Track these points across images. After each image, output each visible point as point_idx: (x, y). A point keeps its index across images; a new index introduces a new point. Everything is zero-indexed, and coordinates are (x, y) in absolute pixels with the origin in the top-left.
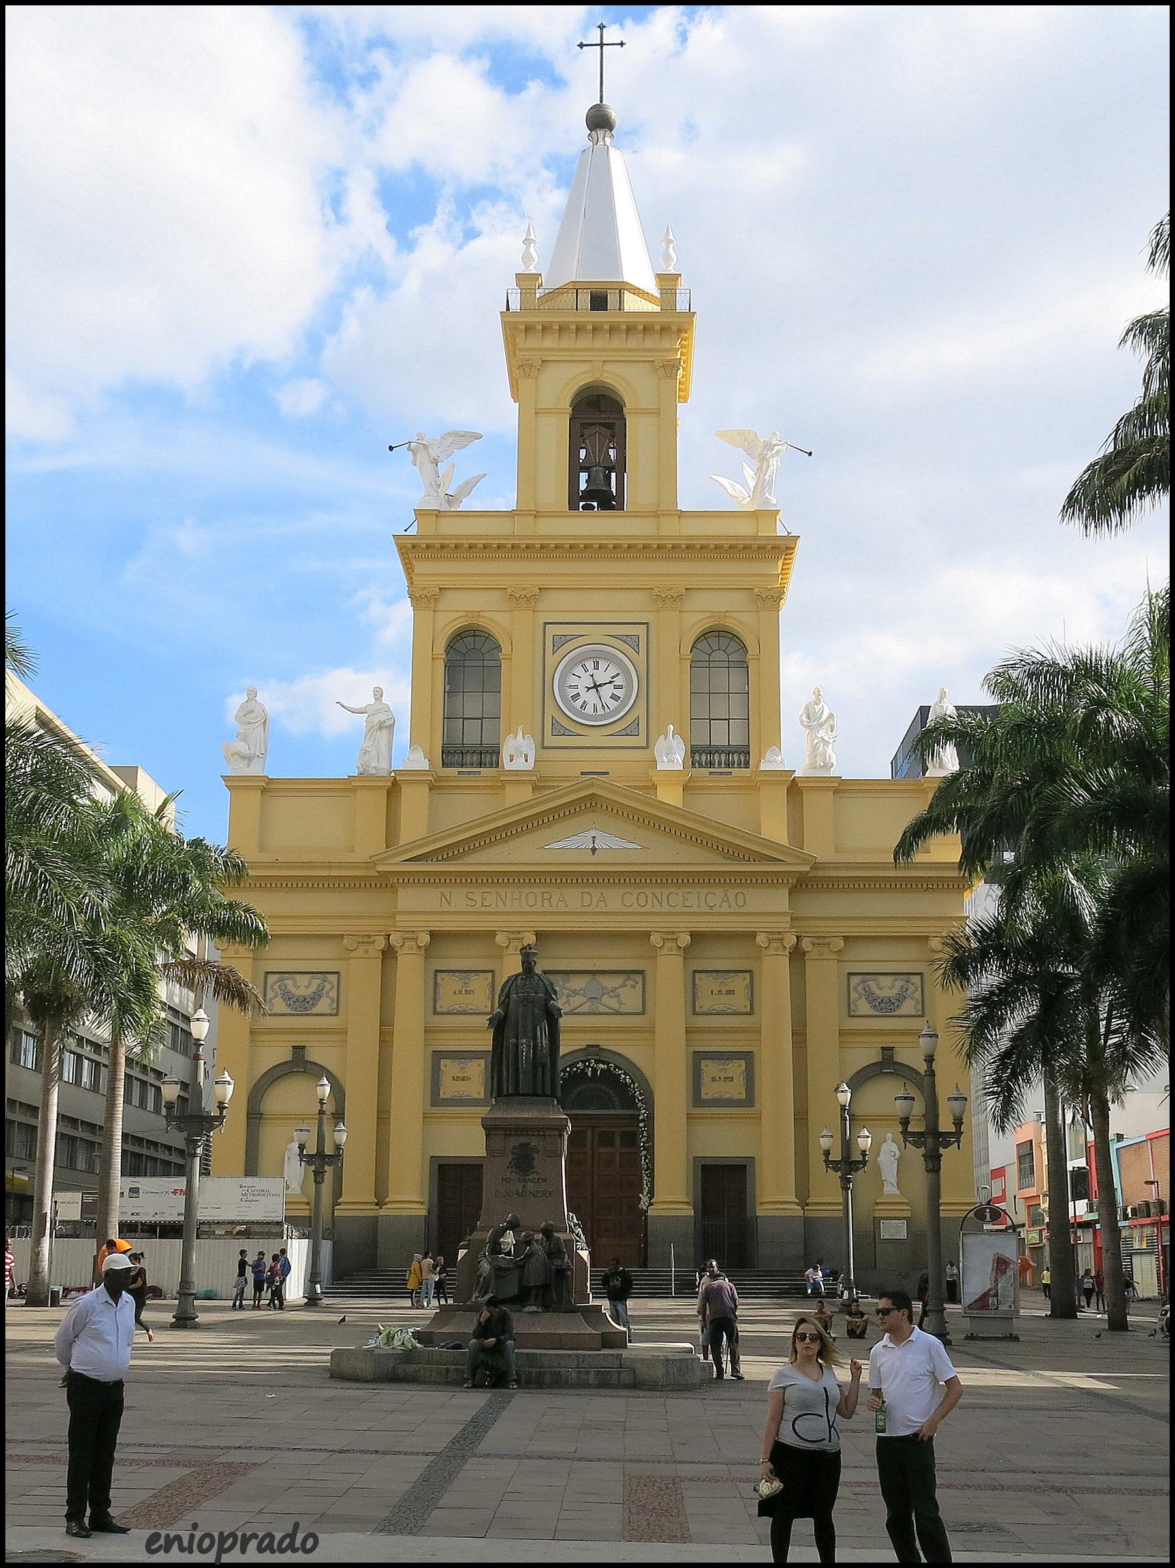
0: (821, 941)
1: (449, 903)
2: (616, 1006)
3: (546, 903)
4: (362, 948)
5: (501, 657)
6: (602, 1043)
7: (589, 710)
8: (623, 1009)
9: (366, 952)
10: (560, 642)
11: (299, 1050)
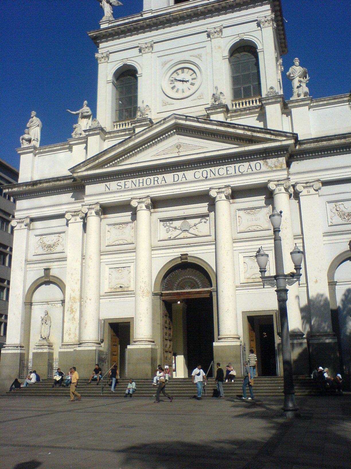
0: (308, 185)
1: (109, 189)
2: (197, 233)
3: (156, 182)
4: (74, 218)
5: (138, 76)
6: (190, 254)
7: (180, 91)
8: (200, 234)
9: (76, 220)
10: (165, 63)
11: (47, 270)
